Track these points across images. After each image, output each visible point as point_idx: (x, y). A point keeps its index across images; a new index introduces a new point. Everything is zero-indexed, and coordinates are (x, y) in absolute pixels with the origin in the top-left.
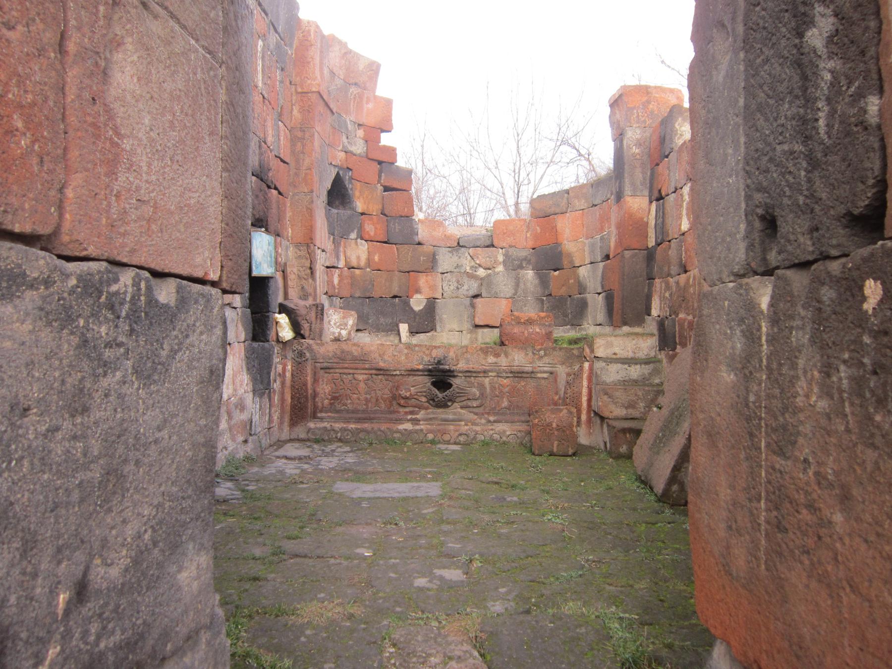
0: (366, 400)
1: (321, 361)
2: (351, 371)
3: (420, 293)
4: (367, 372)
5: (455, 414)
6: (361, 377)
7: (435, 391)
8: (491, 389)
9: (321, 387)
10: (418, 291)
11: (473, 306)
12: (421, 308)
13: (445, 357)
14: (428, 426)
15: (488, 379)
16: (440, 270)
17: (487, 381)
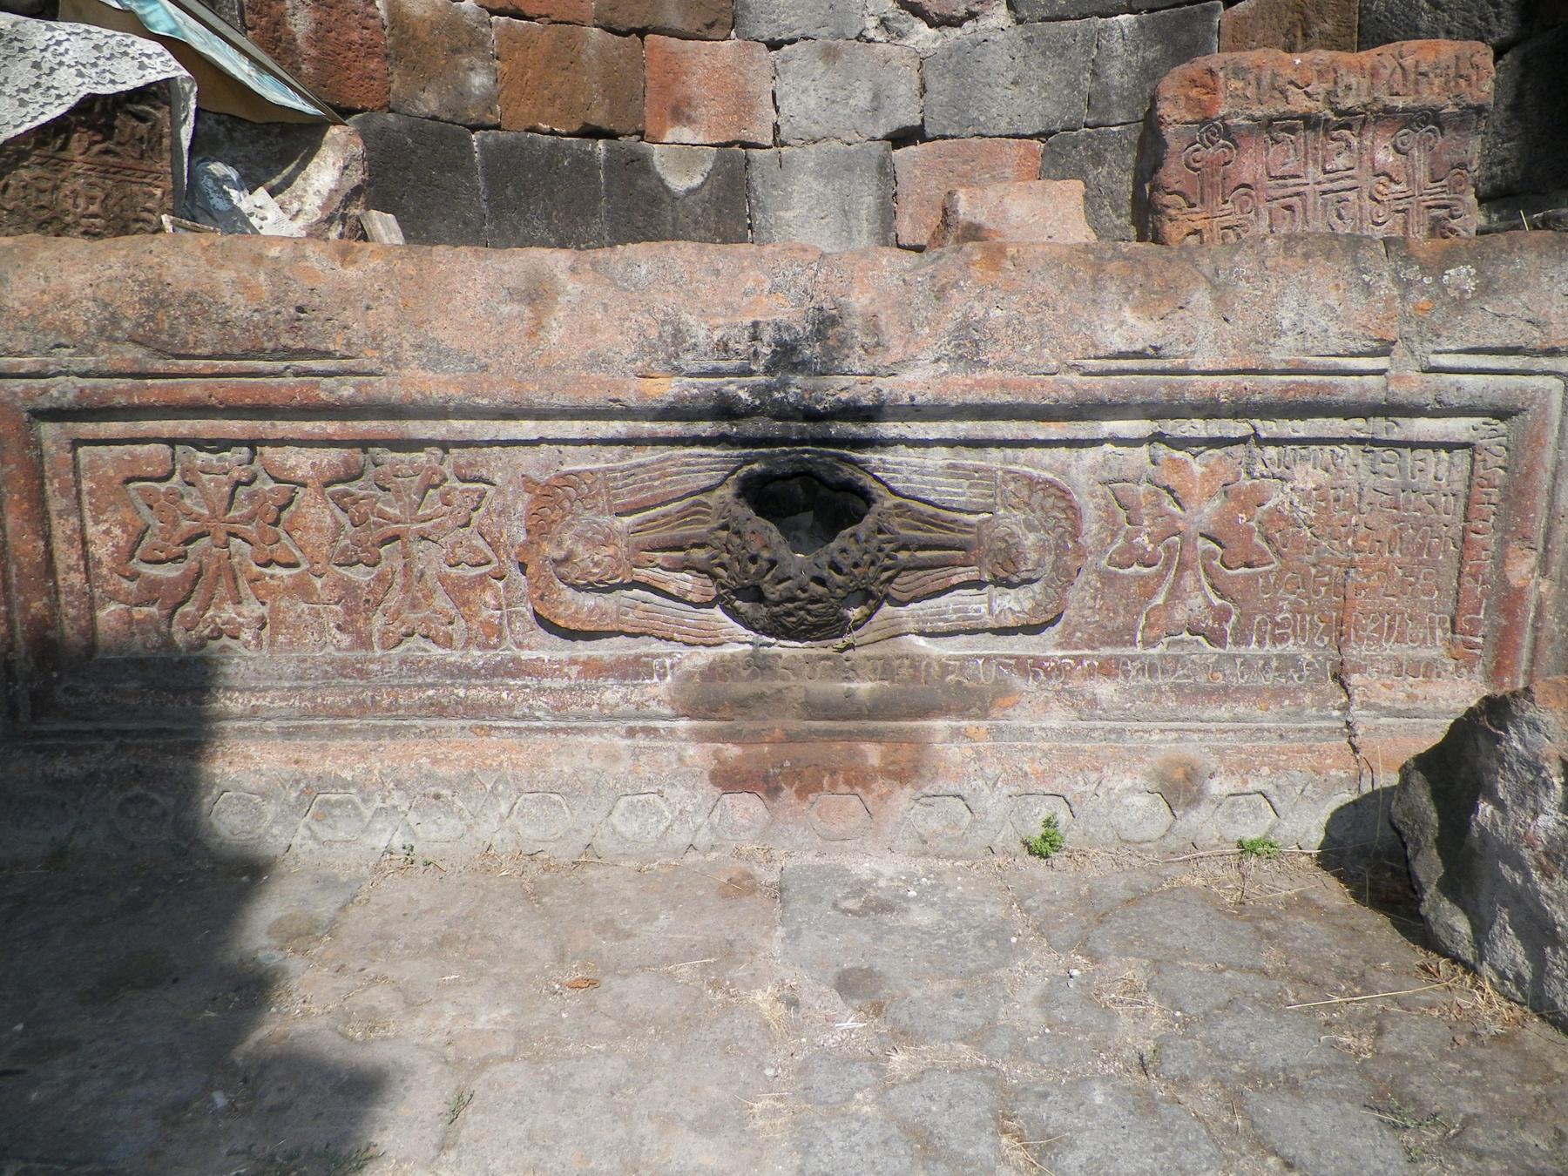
0: (349, 589)
1: (29, 363)
2: (235, 427)
3: (690, 121)
4: (331, 428)
5: (885, 669)
6: (300, 462)
7: (764, 535)
8: (1109, 520)
9: (62, 528)
10: (680, 113)
11: (886, 172)
12: (698, 180)
13: (826, 323)
14: (732, 751)
15: (1090, 455)
16: (767, 32)
17: (1081, 469)
